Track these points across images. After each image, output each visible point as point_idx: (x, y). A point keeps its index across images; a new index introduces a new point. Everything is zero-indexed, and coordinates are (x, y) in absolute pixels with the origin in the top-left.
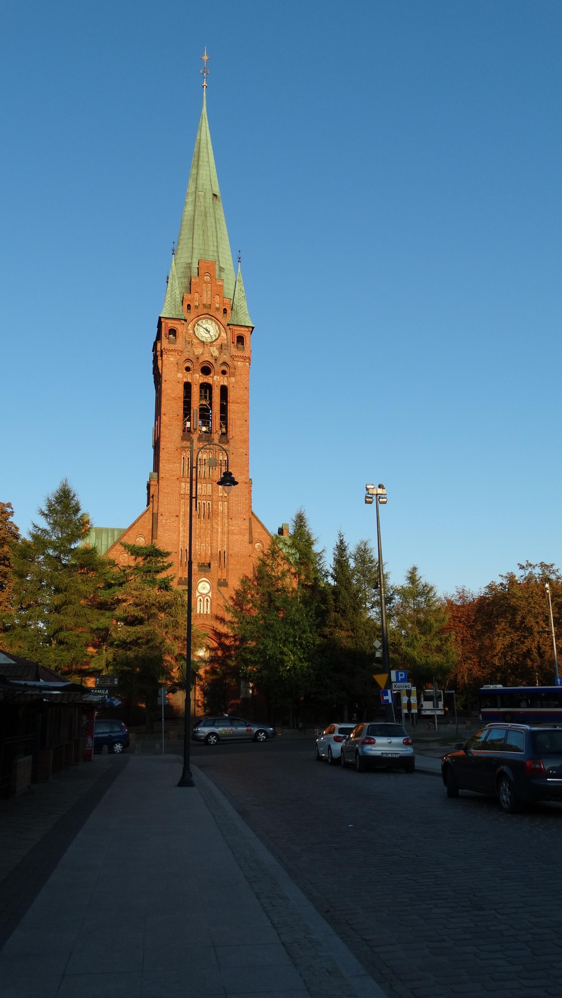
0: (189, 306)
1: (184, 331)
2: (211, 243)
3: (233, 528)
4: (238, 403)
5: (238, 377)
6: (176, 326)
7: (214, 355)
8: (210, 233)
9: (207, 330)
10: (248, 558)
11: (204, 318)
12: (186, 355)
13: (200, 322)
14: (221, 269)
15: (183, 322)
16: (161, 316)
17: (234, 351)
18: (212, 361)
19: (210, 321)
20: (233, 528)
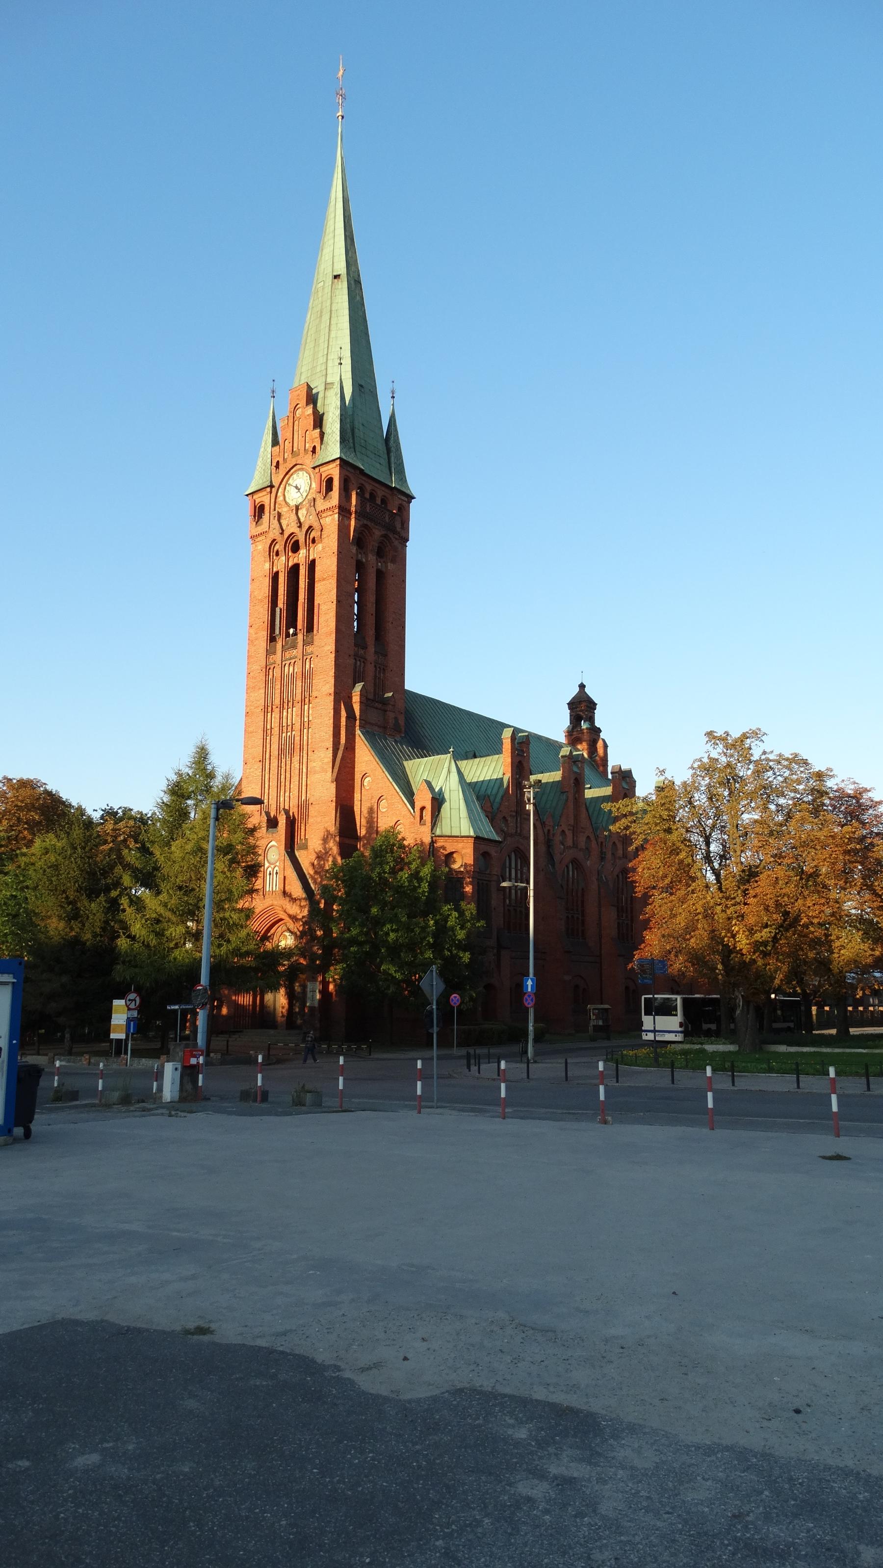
0: (278, 462)
1: (273, 500)
2: (320, 354)
3: (314, 764)
4: (324, 579)
5: (325, 541)
6: (263, 499)
7: (302, 520)
8: (322, 340)
9: (296, 487)
10: (329, 804)
11: (295, 471)
12: (271, 536)
13: (290, 481)
14: (327, 386)
15: (268, 489)
16: (247, 493)
17: (321, 505)
18: (296, 530)
19: (301, 473)
20: (314, 764)
